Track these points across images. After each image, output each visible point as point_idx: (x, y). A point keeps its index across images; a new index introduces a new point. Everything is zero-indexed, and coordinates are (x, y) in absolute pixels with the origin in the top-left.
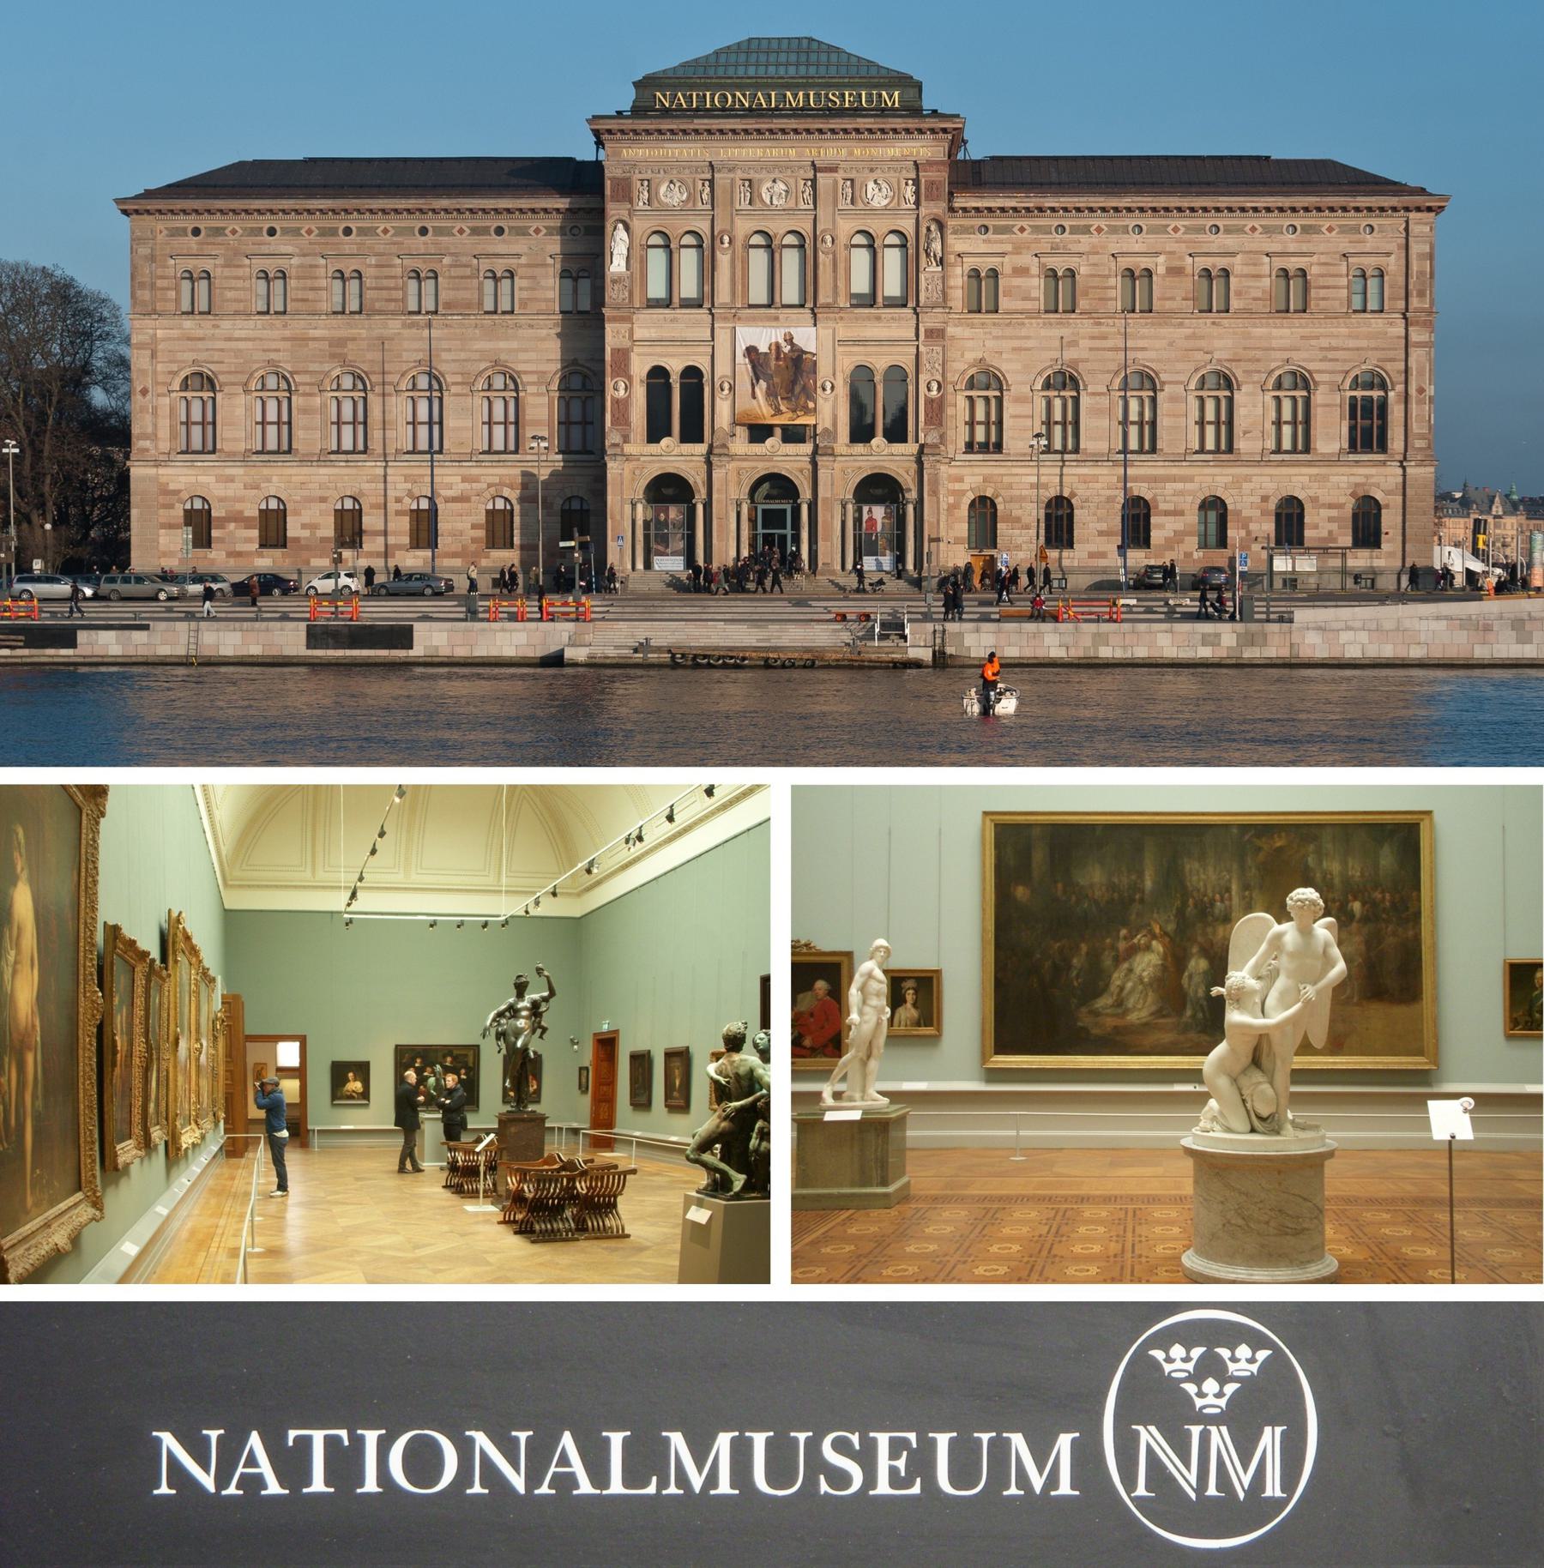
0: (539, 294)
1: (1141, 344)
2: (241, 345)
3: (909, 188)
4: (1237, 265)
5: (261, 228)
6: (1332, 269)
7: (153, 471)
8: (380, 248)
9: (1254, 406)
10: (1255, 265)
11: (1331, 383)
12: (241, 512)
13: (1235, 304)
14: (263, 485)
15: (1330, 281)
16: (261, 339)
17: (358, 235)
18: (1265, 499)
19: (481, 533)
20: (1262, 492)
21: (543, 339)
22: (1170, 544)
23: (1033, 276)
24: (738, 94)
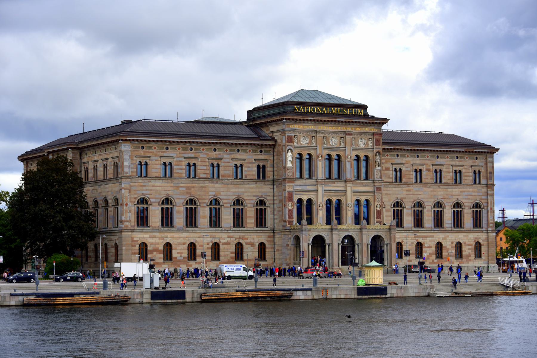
0: (250, 173)
1: (419, 193)
2: (158, 188)
3: (370, 142)
4: (444, 169)
5: (164, 147)
6: (468, 171)
7: (130, 233)
8: (201, 156)
9: (449, 213)
10: (448, 168)
11: (468, 206)
12: (158, 248)
13: (444, 181)
14: (165, 238)
15: (467, 174)
16: (164, 187)
17: (194, 151)
18: (452, 243)
19: (234, 255)
20: (451, 241)
21: (252, 188)
22: (428, 257)
23: (390, 171)
24: (318, 108)
